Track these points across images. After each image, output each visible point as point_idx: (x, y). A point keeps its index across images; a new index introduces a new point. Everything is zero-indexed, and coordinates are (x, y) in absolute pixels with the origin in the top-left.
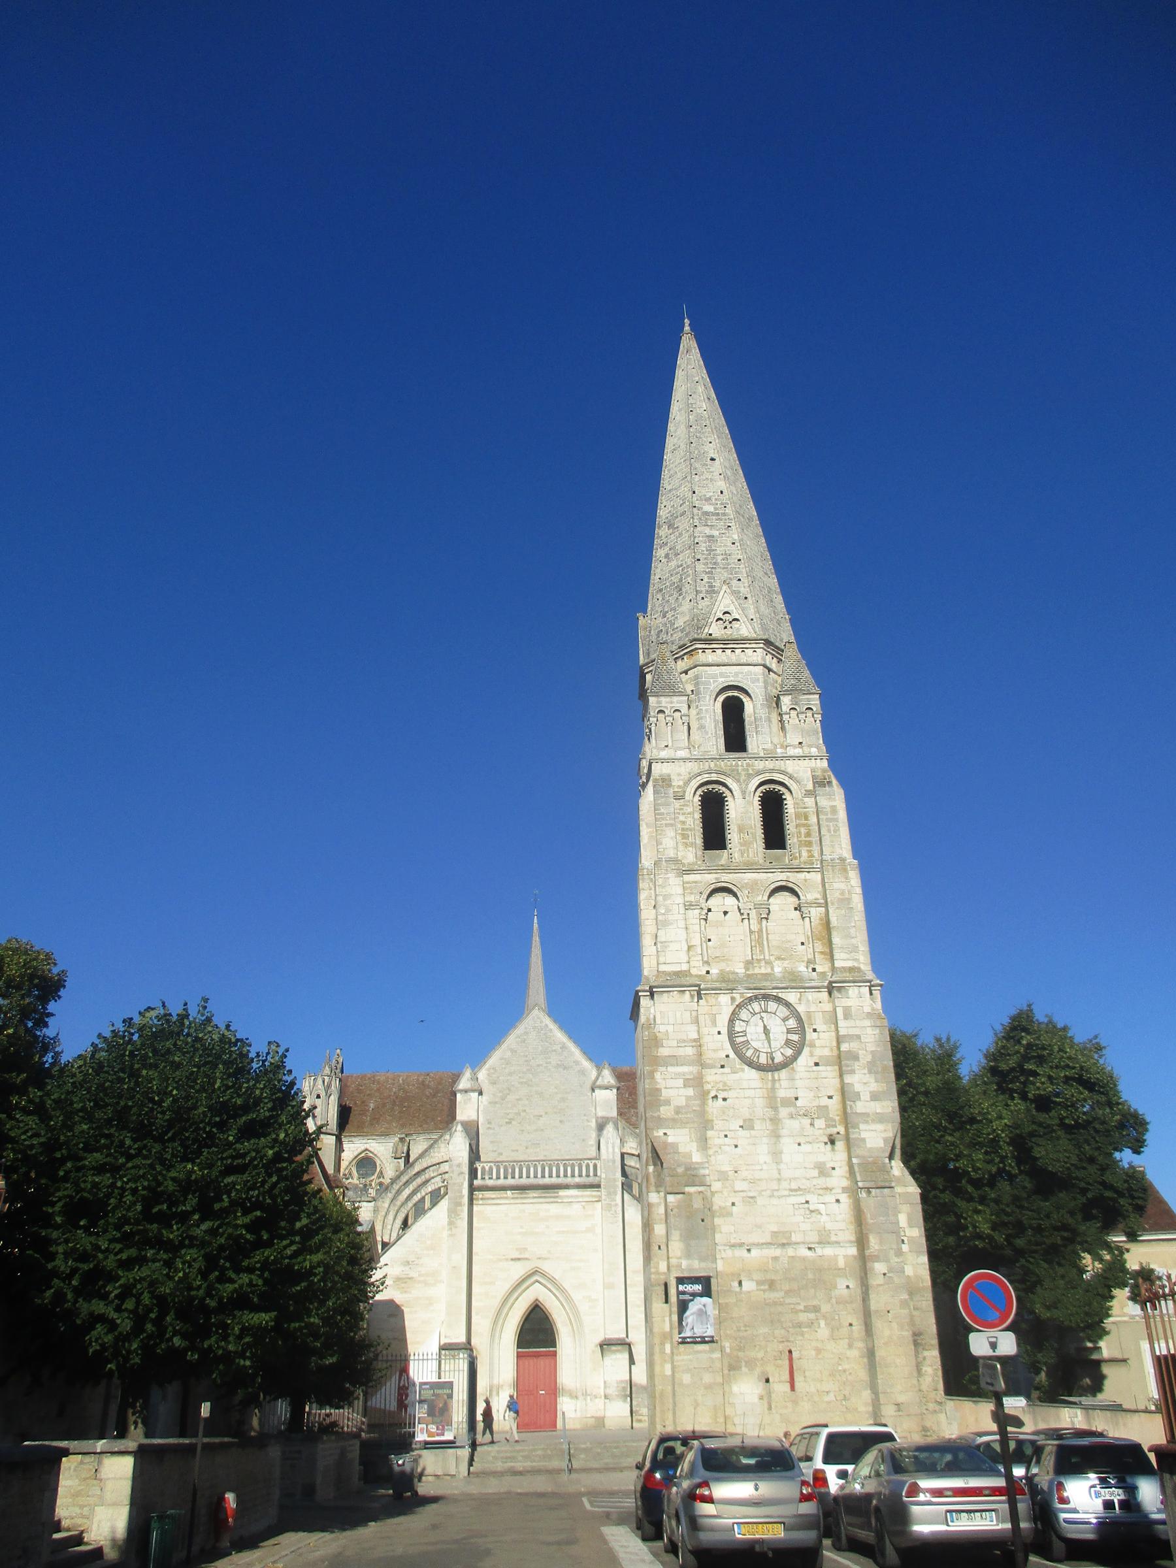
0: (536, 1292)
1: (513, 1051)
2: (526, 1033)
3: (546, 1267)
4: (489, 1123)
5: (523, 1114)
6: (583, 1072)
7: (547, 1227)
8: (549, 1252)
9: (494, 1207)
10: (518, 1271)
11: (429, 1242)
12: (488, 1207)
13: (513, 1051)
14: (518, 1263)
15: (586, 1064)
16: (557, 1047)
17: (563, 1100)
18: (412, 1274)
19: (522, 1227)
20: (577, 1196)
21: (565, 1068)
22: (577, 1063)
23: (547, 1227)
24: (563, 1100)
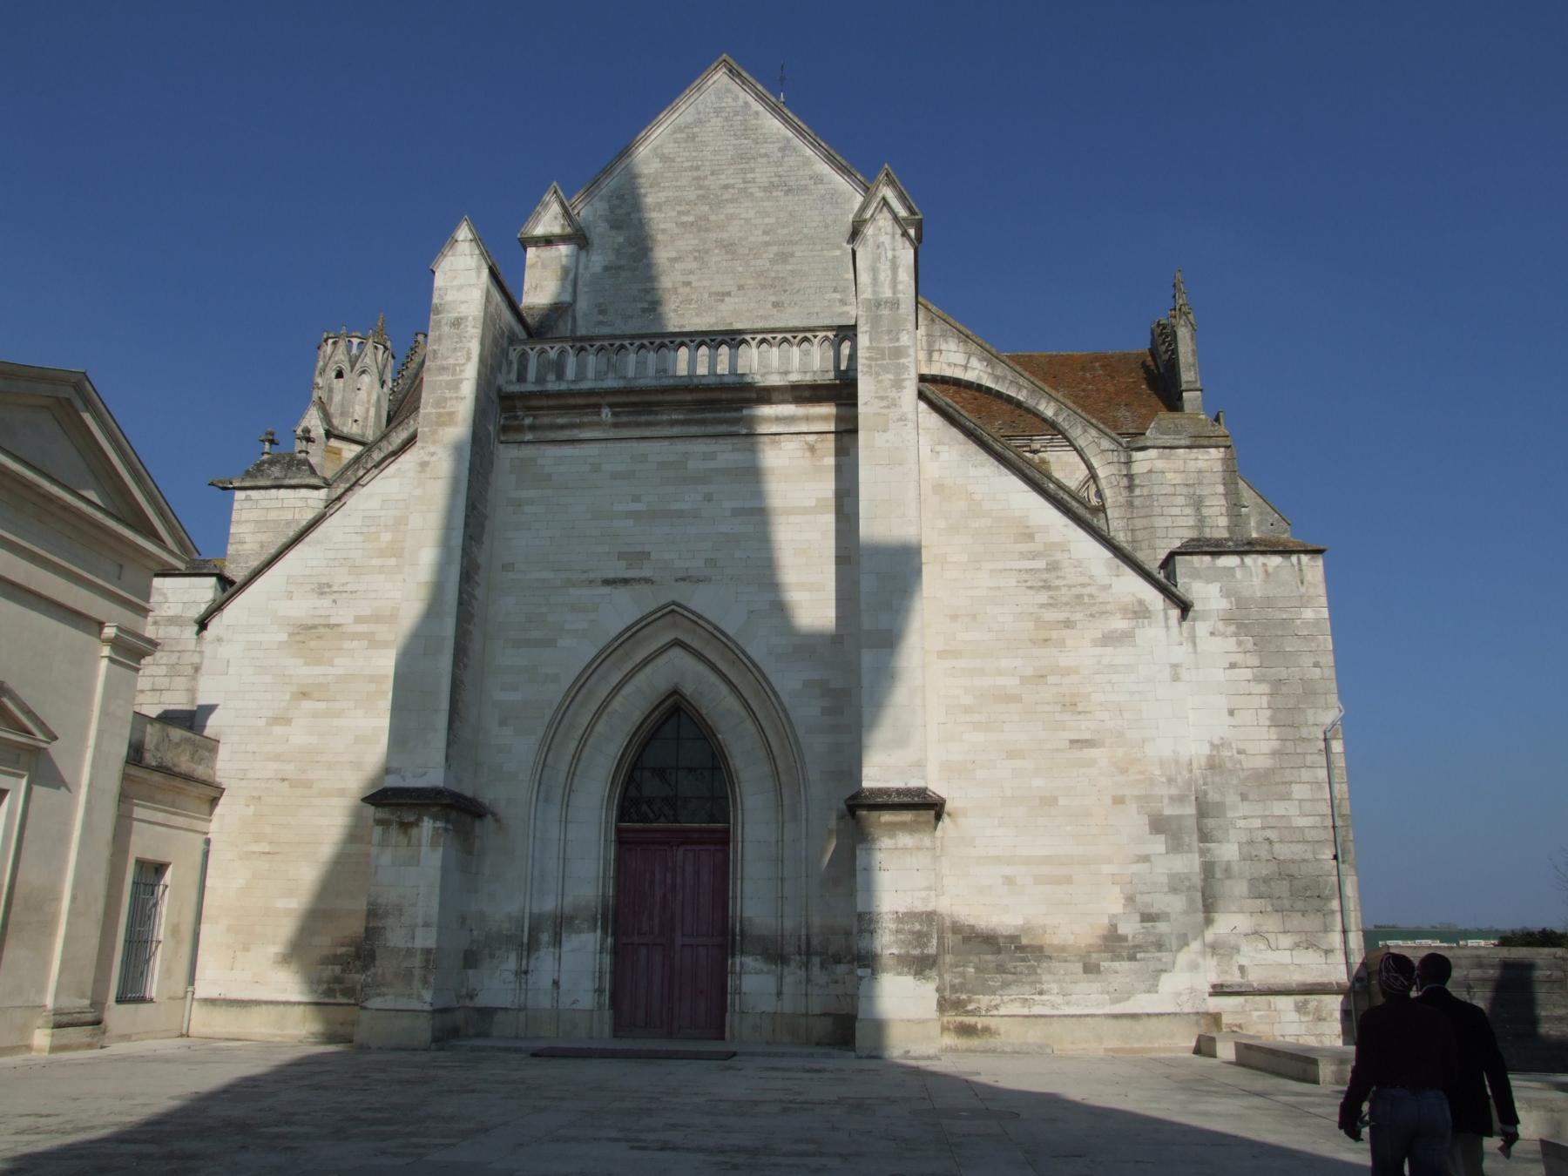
0: (678, 670)
1: (665, 159)
2: (700, 122)
3: (701, 600)
4: (601, 312)
5: (684, 291)
6: (833, 197)
7: (709, 498)
8: (711, 562)
9: (567, 450)
10: (621, 610)
11: (387, 537)
12: (552, 451)
13: (665, 159)
14: (622, 593)
15: (840, 182)
16: (772, 148)
17: (782, 258)
18: (344, 615)
19: (636, 499)
20: (791, 419)
21: (789, 191)
22: (818, 179)
23: (709, 498)
24: (782, 258)
